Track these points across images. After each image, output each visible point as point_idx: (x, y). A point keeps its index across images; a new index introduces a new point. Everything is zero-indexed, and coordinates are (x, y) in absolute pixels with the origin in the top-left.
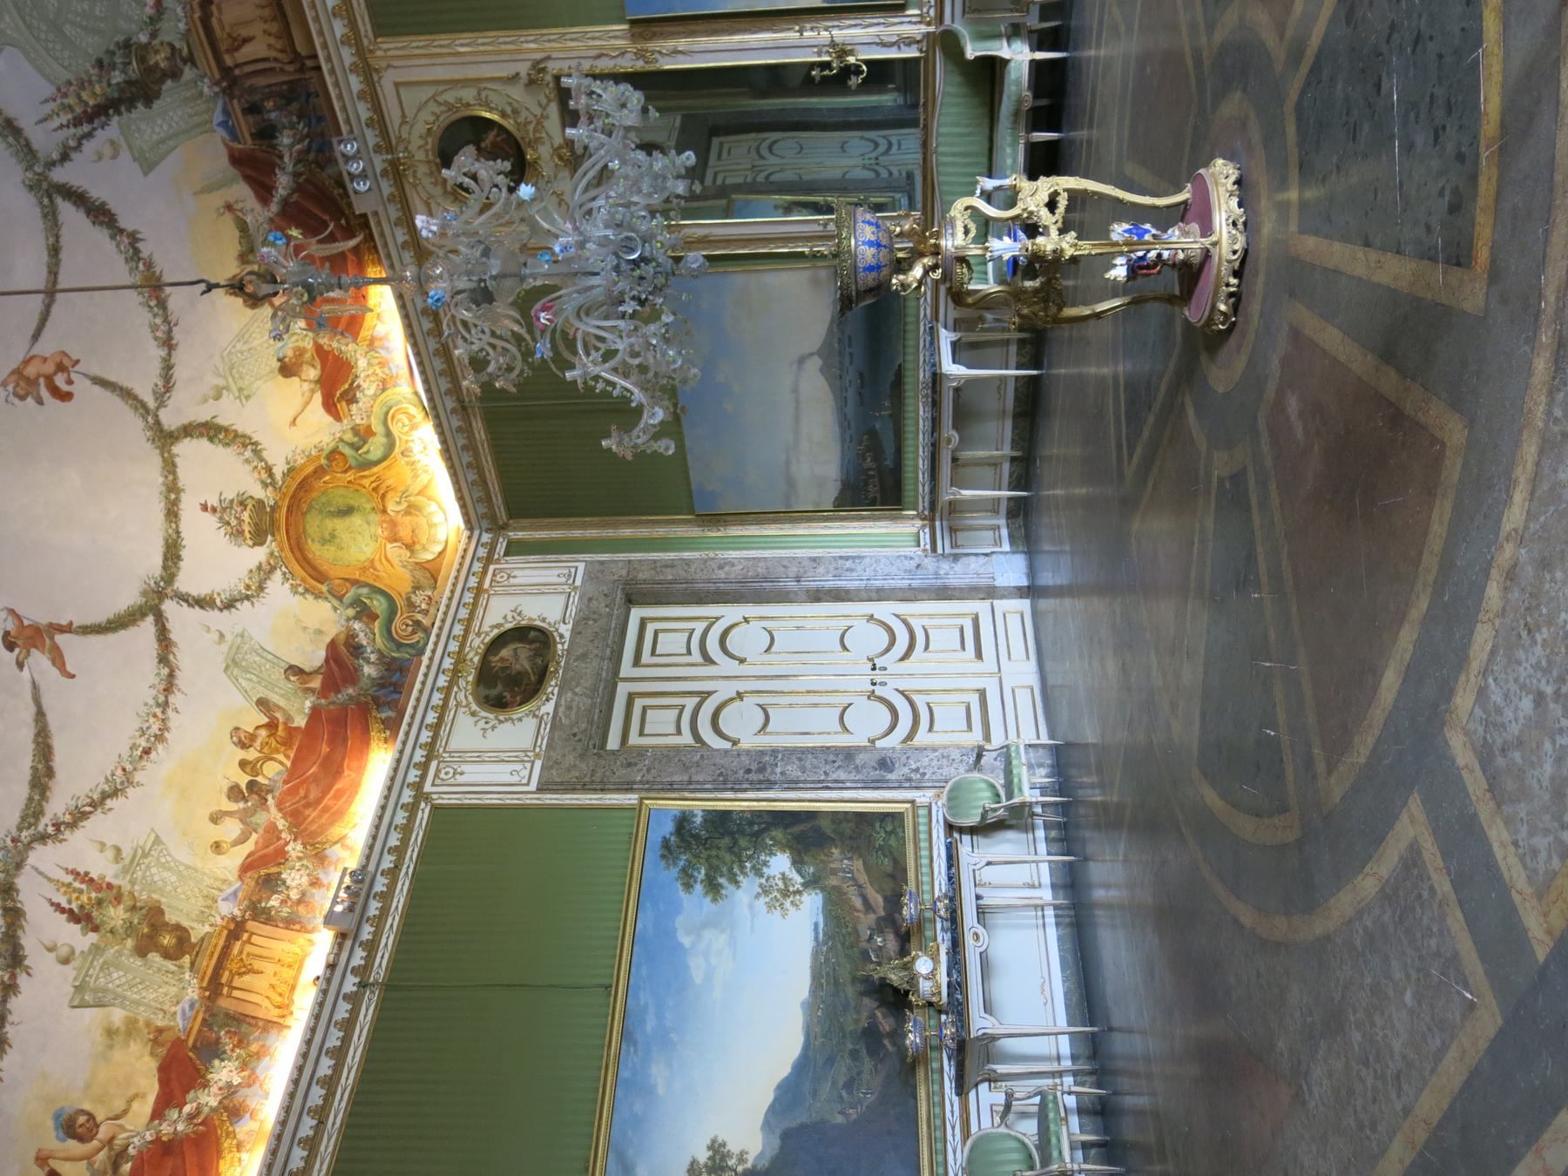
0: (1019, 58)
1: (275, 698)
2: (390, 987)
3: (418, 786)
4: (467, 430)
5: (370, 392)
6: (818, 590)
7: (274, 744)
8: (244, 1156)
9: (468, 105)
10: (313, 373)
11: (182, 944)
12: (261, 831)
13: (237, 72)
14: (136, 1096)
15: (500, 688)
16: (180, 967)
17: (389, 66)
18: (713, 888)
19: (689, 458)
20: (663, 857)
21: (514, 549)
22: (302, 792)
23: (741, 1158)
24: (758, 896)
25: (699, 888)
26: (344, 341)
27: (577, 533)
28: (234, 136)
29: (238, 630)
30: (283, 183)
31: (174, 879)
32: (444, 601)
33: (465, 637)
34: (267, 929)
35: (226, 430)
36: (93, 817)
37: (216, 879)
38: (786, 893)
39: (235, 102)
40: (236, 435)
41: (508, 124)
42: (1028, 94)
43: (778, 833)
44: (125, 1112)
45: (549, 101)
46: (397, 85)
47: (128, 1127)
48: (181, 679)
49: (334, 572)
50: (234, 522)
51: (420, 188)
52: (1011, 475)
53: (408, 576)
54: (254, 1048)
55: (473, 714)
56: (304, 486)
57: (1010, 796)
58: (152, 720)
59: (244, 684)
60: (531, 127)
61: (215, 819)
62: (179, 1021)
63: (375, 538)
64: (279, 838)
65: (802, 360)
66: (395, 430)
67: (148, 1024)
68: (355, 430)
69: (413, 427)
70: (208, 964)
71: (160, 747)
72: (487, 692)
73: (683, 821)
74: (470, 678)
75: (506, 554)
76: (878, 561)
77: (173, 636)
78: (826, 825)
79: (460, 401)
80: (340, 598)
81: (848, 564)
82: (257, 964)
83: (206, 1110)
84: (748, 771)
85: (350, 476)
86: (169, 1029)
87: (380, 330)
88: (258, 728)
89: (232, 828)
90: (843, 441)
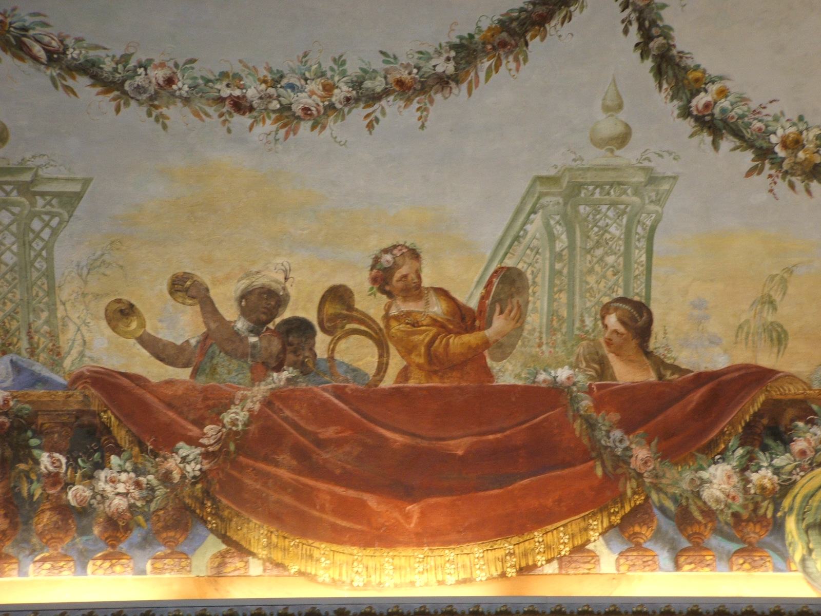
7: (422, 339)
12: (202, 382)
22: (330, 432)
29: (663, 167)
36: (27, 66)
37: (53, 336)
48: (446, 106)
58: (315, 86)
59: (535, 226)
61: (183, 287)
64: (200, 423)
71: (269, 126)
77: (535, 44)
88: (442, 293)
89: (184, 326)
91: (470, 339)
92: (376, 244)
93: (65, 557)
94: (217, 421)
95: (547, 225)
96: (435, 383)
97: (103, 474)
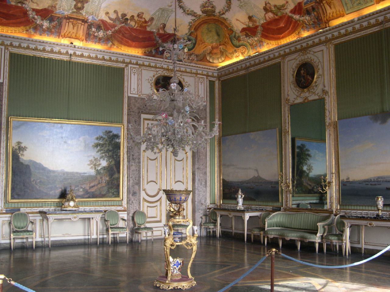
0: (317, 239)
1: (154, 22)
2: (70, 62)
3: (130, 63)
4: (241, 69)
5: (249, 41)
6: (195, 174)
8: (25, 32)
9: (318, 72)
10: (251, 25)
11: (79, 9)
12: (114, 23)
13: (322, 4)
14: (38, 4)
15: (162, 83)
16: (73, 9)
17: (327, 48)
18: (97, 145)
19: (234, 136)
20: (106, 131)
21: (212, 84)
22: (127, 32)
23: (22, 155)
24: (94, 157)
25: (97, 141)
26: (261, 34)
27: (217, 101)
28: (306, 3)
30: (297, 17)
31: (96, 4)
32: (191, 64)
33: (180, 71)
34: (86, 29)
35: (230, 2)
37: (98, 14)
38: (95, 165)
39: (314, 4)
40: (230, 5)
41: (313, 84)
42: (307, 241)
43: (113, 163)
44: (33, 2)
45: (319, 96)
46: (323, 50)
47: (30, 4)
49: (199, 33)
50: (207, 5)
51: (298, 57)
52: (229, 232)
53: (201, 53)
54: (53, 30)
55: (154, 76)
56: (222, 23)
57: (111, 228)
60: (313, 90)
62: (58, 11)
63: (212, 43)
64: (112, 28)
65: (257, 171)
66: (240, 48)
67: (56, 4)
68: (239, 37)
69: (242, 53)
70: (74, 16)
72: (161, 79)
73: (117, 136)
74: (166, 74)
75: (209, 80)
76: (205, 191)
78: (116, 176)
79: (249, 67)
80: (190, 35)
81: (203, 183)
82: (76, 28)
83: (36, 21)
84: (133, 155)
85: (227, 35)
86: (56, 9)
87: (265, 44)
88: (144, 18)
89: (113, 16)
90: (238, 182)
91: (146, 24)
92: (139, 11)
93: (93, 42)
94: (114, 28)
95: (159, 14)
96: (140, 29)
97: (100, 32)
